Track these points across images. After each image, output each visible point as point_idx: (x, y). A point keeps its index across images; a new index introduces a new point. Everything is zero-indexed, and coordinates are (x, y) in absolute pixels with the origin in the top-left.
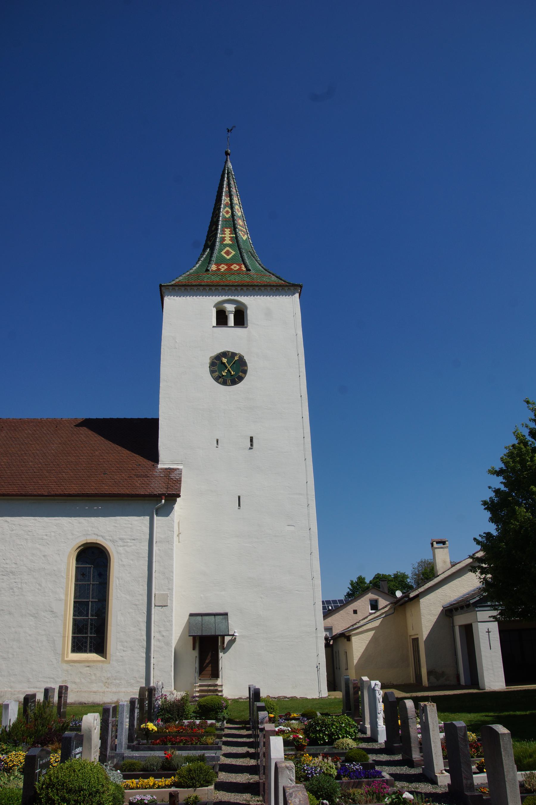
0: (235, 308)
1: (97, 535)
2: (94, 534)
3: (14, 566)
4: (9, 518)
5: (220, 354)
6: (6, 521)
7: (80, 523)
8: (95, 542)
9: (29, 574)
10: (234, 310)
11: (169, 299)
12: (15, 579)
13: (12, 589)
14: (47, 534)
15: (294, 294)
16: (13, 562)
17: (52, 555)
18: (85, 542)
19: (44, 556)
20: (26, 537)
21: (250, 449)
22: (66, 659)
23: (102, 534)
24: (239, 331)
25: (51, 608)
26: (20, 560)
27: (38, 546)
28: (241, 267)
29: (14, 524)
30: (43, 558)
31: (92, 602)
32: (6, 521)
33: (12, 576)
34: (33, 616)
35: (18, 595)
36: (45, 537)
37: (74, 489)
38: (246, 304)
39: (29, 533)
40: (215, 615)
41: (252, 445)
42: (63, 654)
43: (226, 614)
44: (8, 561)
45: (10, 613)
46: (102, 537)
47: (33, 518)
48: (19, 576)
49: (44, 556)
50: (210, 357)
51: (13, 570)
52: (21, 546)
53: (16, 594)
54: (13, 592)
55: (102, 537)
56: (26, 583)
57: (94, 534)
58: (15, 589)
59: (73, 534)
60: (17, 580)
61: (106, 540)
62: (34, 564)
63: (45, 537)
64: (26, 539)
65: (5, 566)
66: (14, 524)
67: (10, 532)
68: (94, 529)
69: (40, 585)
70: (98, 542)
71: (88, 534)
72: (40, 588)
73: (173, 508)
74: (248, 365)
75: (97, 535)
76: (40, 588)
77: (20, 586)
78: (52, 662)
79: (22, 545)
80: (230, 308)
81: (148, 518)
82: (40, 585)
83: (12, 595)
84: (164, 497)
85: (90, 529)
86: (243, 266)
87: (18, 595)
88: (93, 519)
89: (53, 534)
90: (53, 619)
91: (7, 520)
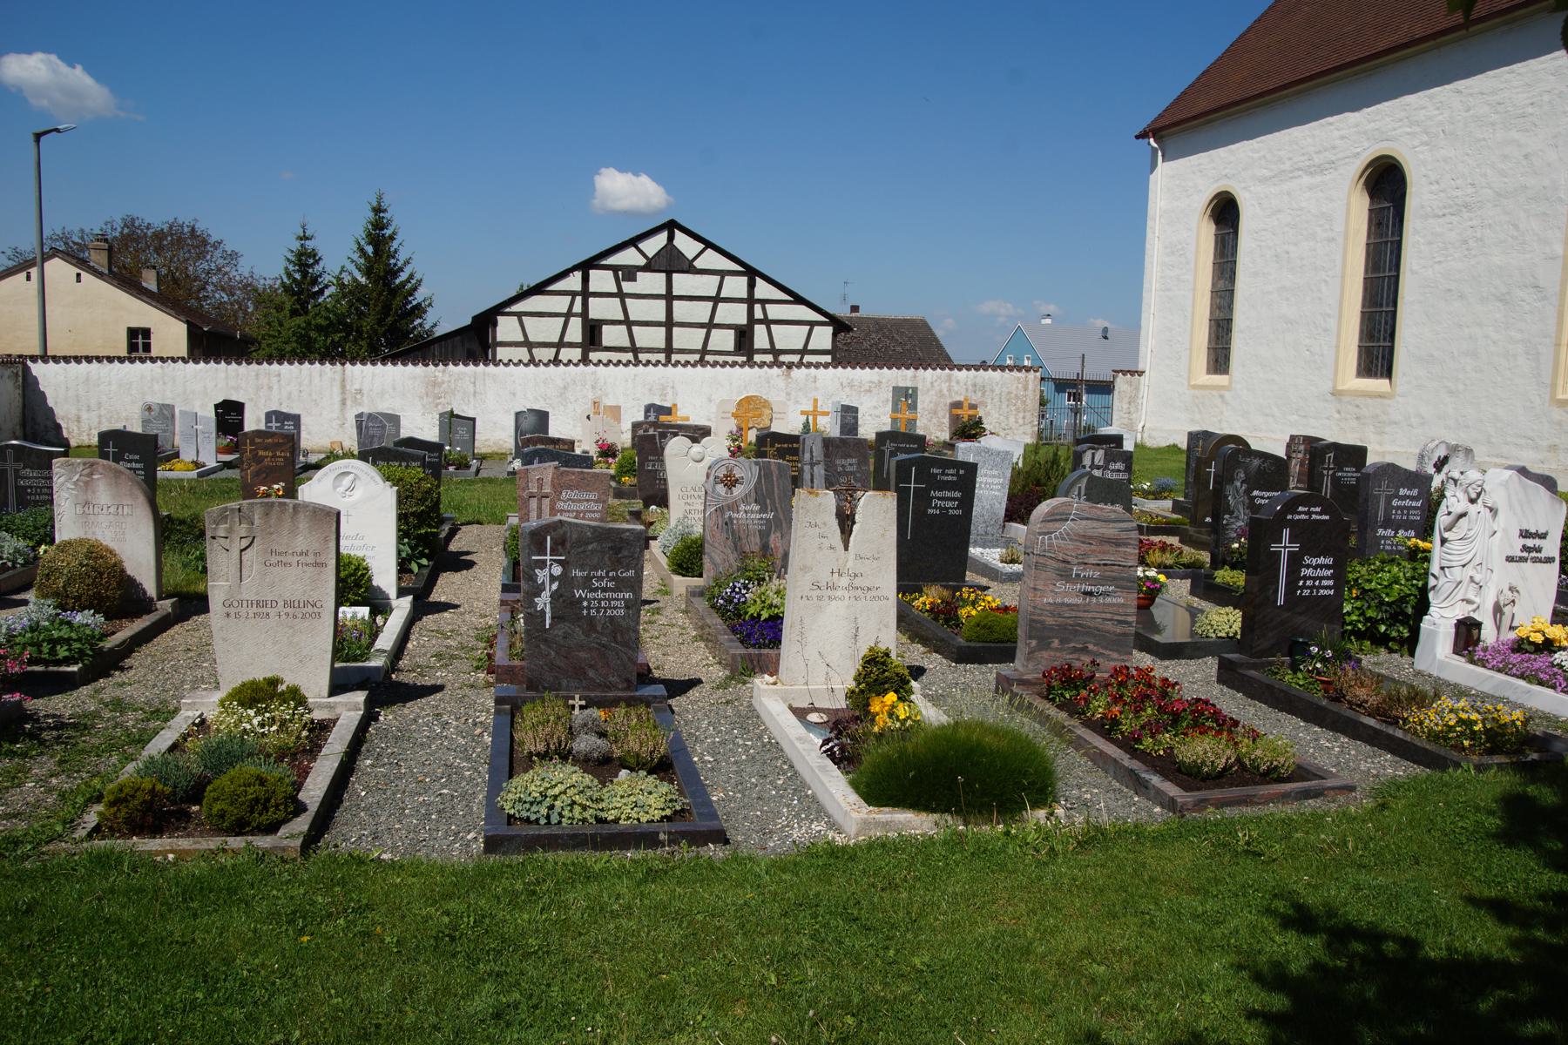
3: (1470, 190)
6: (1459, 92)
9: (1496, 206)
12: (1471, 219)
16: (1469, 181)
17: (1541, 150)
22: (1560, 396)
25: (1535, 278)
26: (1481, 175)
27: (1516, 135)
32: (1459, 92)
33: (1466, 215)
34: (1501, 300)
35: (1475, 256)
42: (1554, 385)
45: (1462, 297)
48: (1479, 213)
51: (1468, 199)
52: (1483, 143)
53: (1473, 252)
54: (1468, 249)
56: (1490, 225)
58: (1471, 242)
60: (1474, 223)
62: (1506, 180)
65: (1455, 194)
67: (1465, 114)
69: (1516, 227)
72: (1515, 234)
76: (1515, 234)
77: (1479, 235)
78: (1532, 402)
79: (1484, 139)
82: (1516, 227)
83: (1466, 257)
87: (1475, 256)
90: (1538, 304)
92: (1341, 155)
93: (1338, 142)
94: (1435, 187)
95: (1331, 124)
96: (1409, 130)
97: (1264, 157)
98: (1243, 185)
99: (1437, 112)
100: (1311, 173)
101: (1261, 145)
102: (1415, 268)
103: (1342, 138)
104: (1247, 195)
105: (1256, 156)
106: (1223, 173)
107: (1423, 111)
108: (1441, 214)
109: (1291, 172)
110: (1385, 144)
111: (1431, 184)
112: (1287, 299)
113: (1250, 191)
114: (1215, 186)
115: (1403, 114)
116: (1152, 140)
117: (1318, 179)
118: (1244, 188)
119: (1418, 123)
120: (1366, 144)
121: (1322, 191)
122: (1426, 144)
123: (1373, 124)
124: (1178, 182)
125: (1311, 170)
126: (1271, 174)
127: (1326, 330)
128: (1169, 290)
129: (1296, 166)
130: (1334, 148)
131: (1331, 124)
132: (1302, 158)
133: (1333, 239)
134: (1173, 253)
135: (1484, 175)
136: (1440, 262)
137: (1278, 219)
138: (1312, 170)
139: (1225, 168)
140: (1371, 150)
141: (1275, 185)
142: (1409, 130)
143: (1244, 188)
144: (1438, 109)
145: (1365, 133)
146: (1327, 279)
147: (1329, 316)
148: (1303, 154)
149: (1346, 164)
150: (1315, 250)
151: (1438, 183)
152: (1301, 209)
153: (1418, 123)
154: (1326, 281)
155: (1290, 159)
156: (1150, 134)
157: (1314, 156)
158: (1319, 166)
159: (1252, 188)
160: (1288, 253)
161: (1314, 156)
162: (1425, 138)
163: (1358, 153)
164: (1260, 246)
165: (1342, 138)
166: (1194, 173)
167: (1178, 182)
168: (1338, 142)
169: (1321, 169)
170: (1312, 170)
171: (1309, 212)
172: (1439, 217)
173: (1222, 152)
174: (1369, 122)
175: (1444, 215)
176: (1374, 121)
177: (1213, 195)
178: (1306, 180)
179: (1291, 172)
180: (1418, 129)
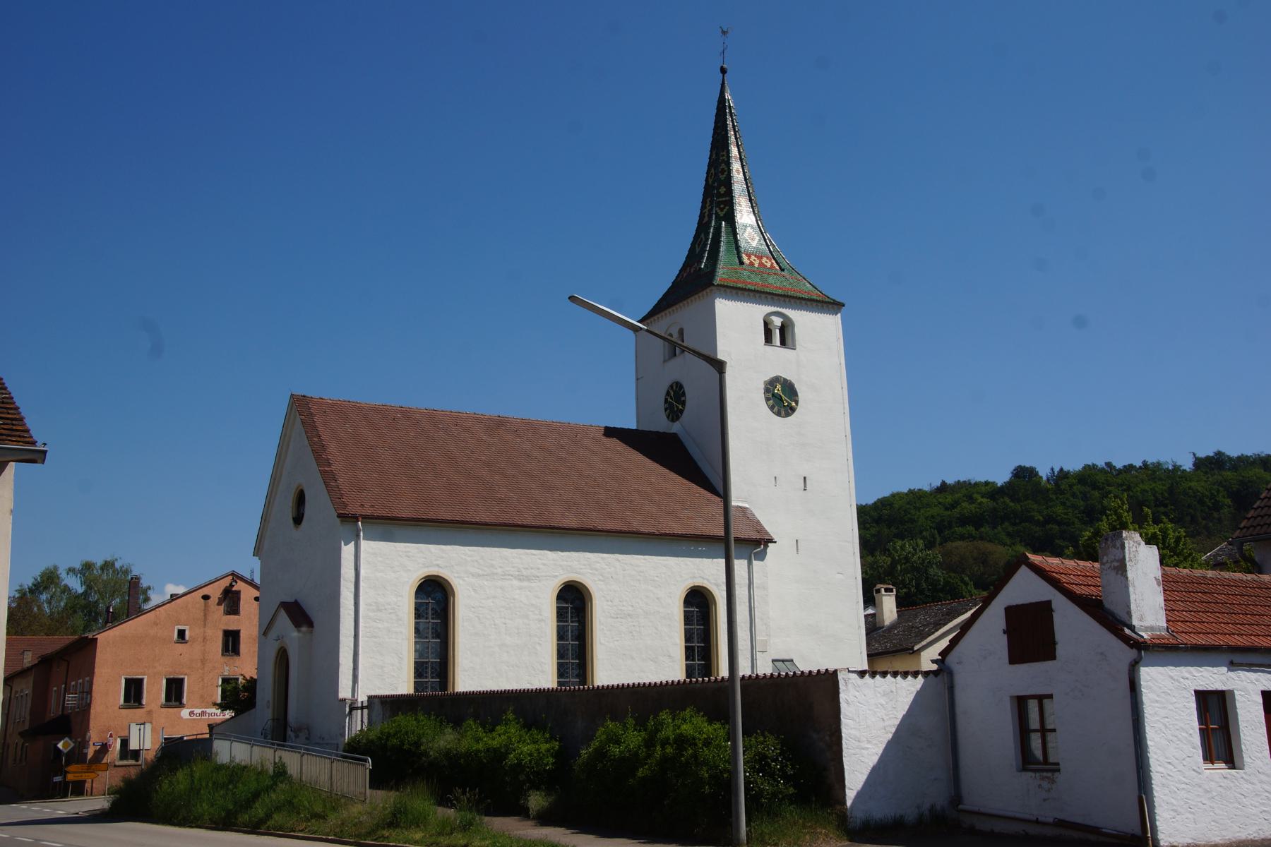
0: (782, 323)
1: (703, 578)
2: (700, 577)
3: (630, 608)
4: (621, 556)
5: (773, 378)
6: (618, 560)
7: (686, 565)
8: (701, 585)
10: (780, 325)
11: (720, 302)
12: (633, 622)
13: (631, 632)
14: (659, 575)
15: (836, 314)
18: (693, 585)
19: (658, 599)
20: (639, 577)
21: (805, 490)
23: (707, 577)
24: (784, 352)
28: (772, 263)
29: (626, 564)
30: (657, 601)
31: (698, 647)
32: (618, 560)
34: (652, 661)
36: (656, 578)
37: (678, 529)
38: (794, 320)
39: (641, 574)
40: (783, 661)
41: (805, 486)
43: (792, 661)
44: (624, 603)
45: (632, 658)
46: (708, 580)
47: (642, 557)
49: (658, 599)
50: (765, 382)
55: (708, 580)
57: (700, 577)
58: (634, 632)
59: (681, 577)
60: (634, 624)
61: (710, 583)
63: (656, 578)
64: (639, 580)
65: (623, 608)
66: (626, 564)
68: (699, 572)
69: (657, 629)
70: (704, 585)
71: (694, 577)
73: (766, 553)
74: (799, 395)
75: (703, 578)
77: (638, 630)
79: (635, 586)
80: (777, 321)
81: (746, 561)
82: (657, 629)
84: (763, 543)
85: (696, 571)
86: (774, 261)
88: (698, 560)
89: (663, 576)
91: (620, 559)
92: (544, 574)
93: (541, 566)
94: (610, 603)
95: (534, 555)
96: (591, 572)
97: (477, 561)
98: (456, 575)
99: (606, 567)
100: (520, 580)
101: (472, 553)
102: (603, 642)
103: (544, 565)
104: (461, 582)
105: (469, 559)
106: (435, 563)
107: (599, 564)
108: (615, 616)
109: (502, 575)
110: (579, 576)
111: (608, 601)
112: (508, 652)
113: (464, 580)
114: (426, 570)
115: (586, 562)
116: (360, 523)
117: (525, 584)
118: (458, 577)
119: (596, 570)
120: (561, 572)
121: (530, 591)
122: (602, 581)
123: (565, 563)
124: (380, 559)
125: (520, 578)
126: (485, 573)
127: (543, 672)
128: (375, 637)
129: (507, 573)
130: (538, 569)
131: (534, 555)
132: (513, 569)
133: (543, 620)
134: (379, 610)
135: (638, 603)
136: (617, 641)
137: (493, 602)
138: (522, 577)
139: (436, 560)
140: (565, 576)
141: (487, 580)
142: (591, 572)
143: (458, 577)
144: (607, 565)
145: (561, 566)
146: (540, 642)
147: (545, 664)
148: (513, 567)
149: (547, 579)
150: (529, 625)
151: (611, 601)
152: (514, 599)
153: (596, 570)
154: (539, 643)
155: (501, 567)
156: (360, 519)
157: (523, 570)
158: (527, 577)
159: (466, 579)
160: (505, 624)
161: (523, 570)
162: (601, 578)
163: (556, 576)
164: (477, 617)
165: (544, 565)
166: (400, 556)
167: (380, 559)
168: (541, 566)
169: (528, 579)
170: (522, 577)
171: (521, 601)
172: (613, 618)
173: (433, 548)
174: (563, 560)
175: (617, 618)
176: (567, 561)
177: (423, 576)
178: (516, 583)
179: (502, 575)
180: (596, 573)
